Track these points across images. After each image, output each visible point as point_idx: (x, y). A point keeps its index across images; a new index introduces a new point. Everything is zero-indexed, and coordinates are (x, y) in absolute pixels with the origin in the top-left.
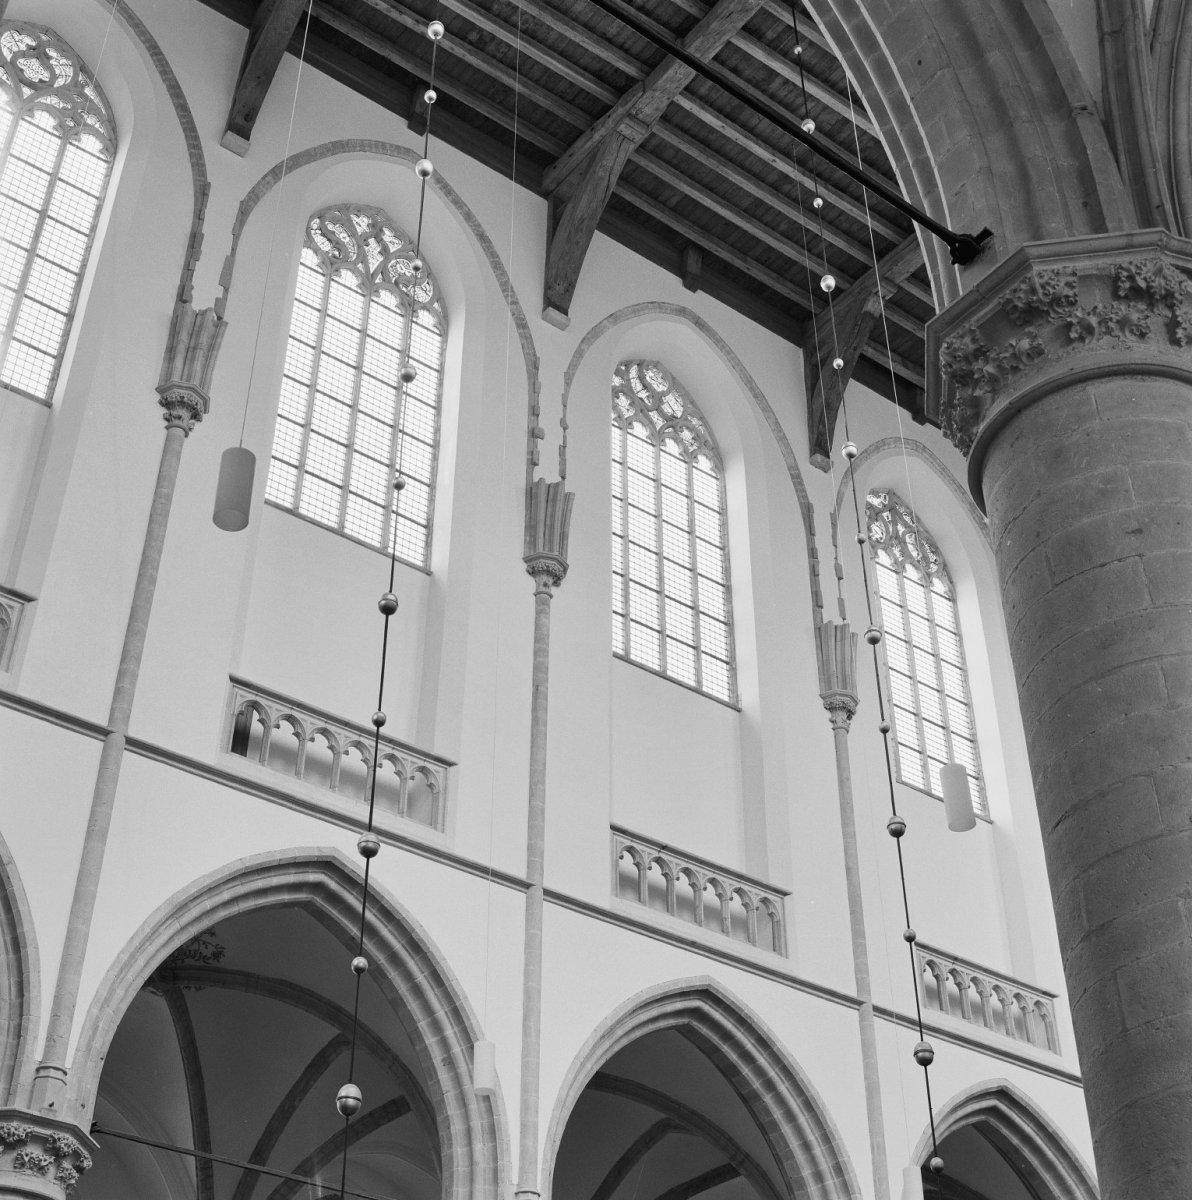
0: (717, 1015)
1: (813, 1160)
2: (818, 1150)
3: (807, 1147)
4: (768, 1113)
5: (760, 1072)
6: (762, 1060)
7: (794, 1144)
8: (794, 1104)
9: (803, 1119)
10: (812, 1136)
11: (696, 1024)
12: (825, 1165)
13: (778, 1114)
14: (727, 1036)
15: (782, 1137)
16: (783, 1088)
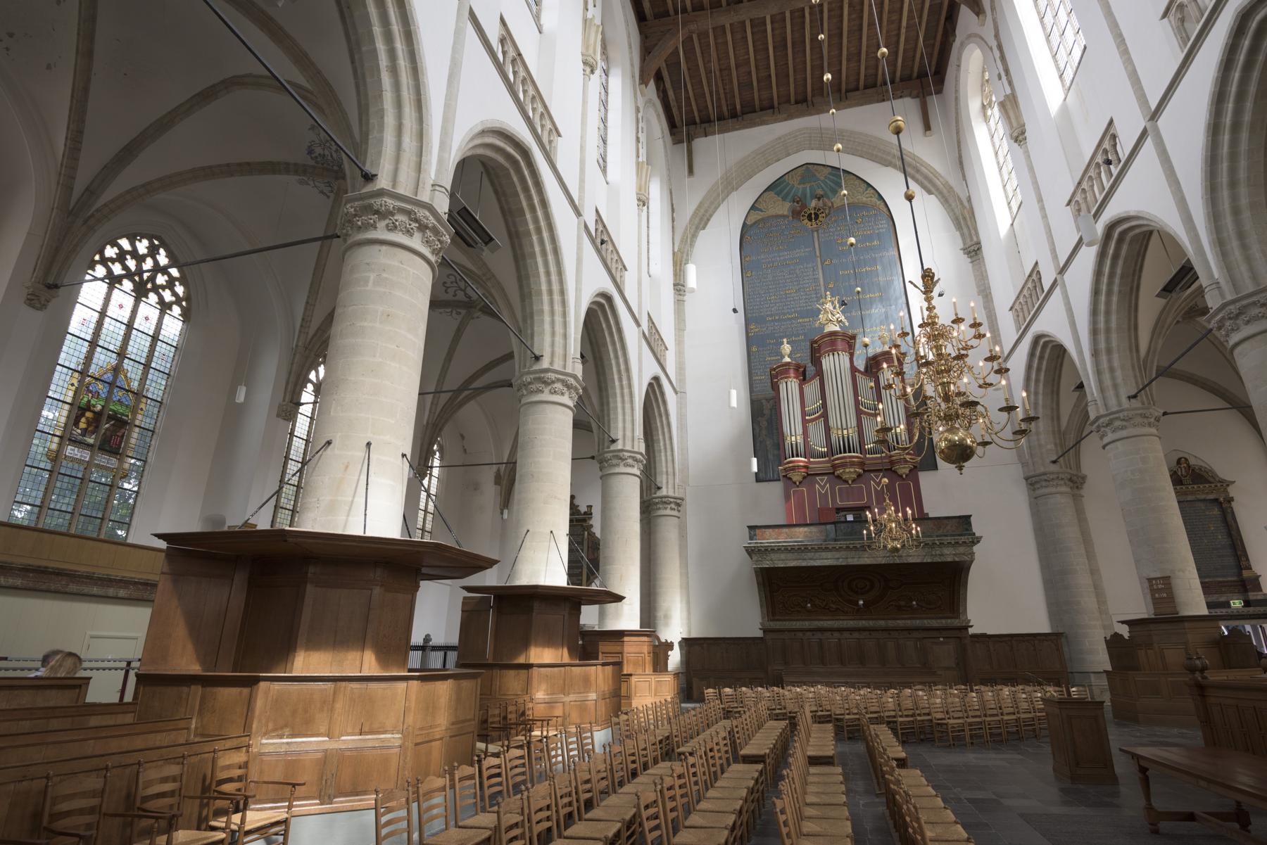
0: (526, 173)
1: (549, 282)
2: (554, 278)
3: (548, 273)
4: (532, 246)
5: (536, 221)
6: (540, 213)
7: (542, 270)
8: (548, 247)
9: (550, 257)
10: (553, 269)
11: (512, 172)
12: (556, 287)
13: (537, 249)
14: (526, 189)
15: (536, 263)
16: (545, 235)
